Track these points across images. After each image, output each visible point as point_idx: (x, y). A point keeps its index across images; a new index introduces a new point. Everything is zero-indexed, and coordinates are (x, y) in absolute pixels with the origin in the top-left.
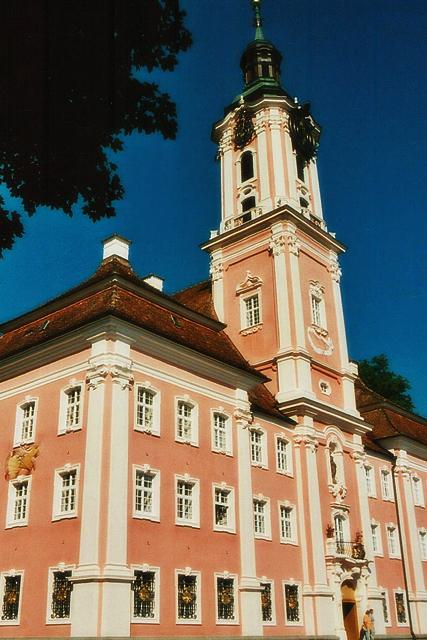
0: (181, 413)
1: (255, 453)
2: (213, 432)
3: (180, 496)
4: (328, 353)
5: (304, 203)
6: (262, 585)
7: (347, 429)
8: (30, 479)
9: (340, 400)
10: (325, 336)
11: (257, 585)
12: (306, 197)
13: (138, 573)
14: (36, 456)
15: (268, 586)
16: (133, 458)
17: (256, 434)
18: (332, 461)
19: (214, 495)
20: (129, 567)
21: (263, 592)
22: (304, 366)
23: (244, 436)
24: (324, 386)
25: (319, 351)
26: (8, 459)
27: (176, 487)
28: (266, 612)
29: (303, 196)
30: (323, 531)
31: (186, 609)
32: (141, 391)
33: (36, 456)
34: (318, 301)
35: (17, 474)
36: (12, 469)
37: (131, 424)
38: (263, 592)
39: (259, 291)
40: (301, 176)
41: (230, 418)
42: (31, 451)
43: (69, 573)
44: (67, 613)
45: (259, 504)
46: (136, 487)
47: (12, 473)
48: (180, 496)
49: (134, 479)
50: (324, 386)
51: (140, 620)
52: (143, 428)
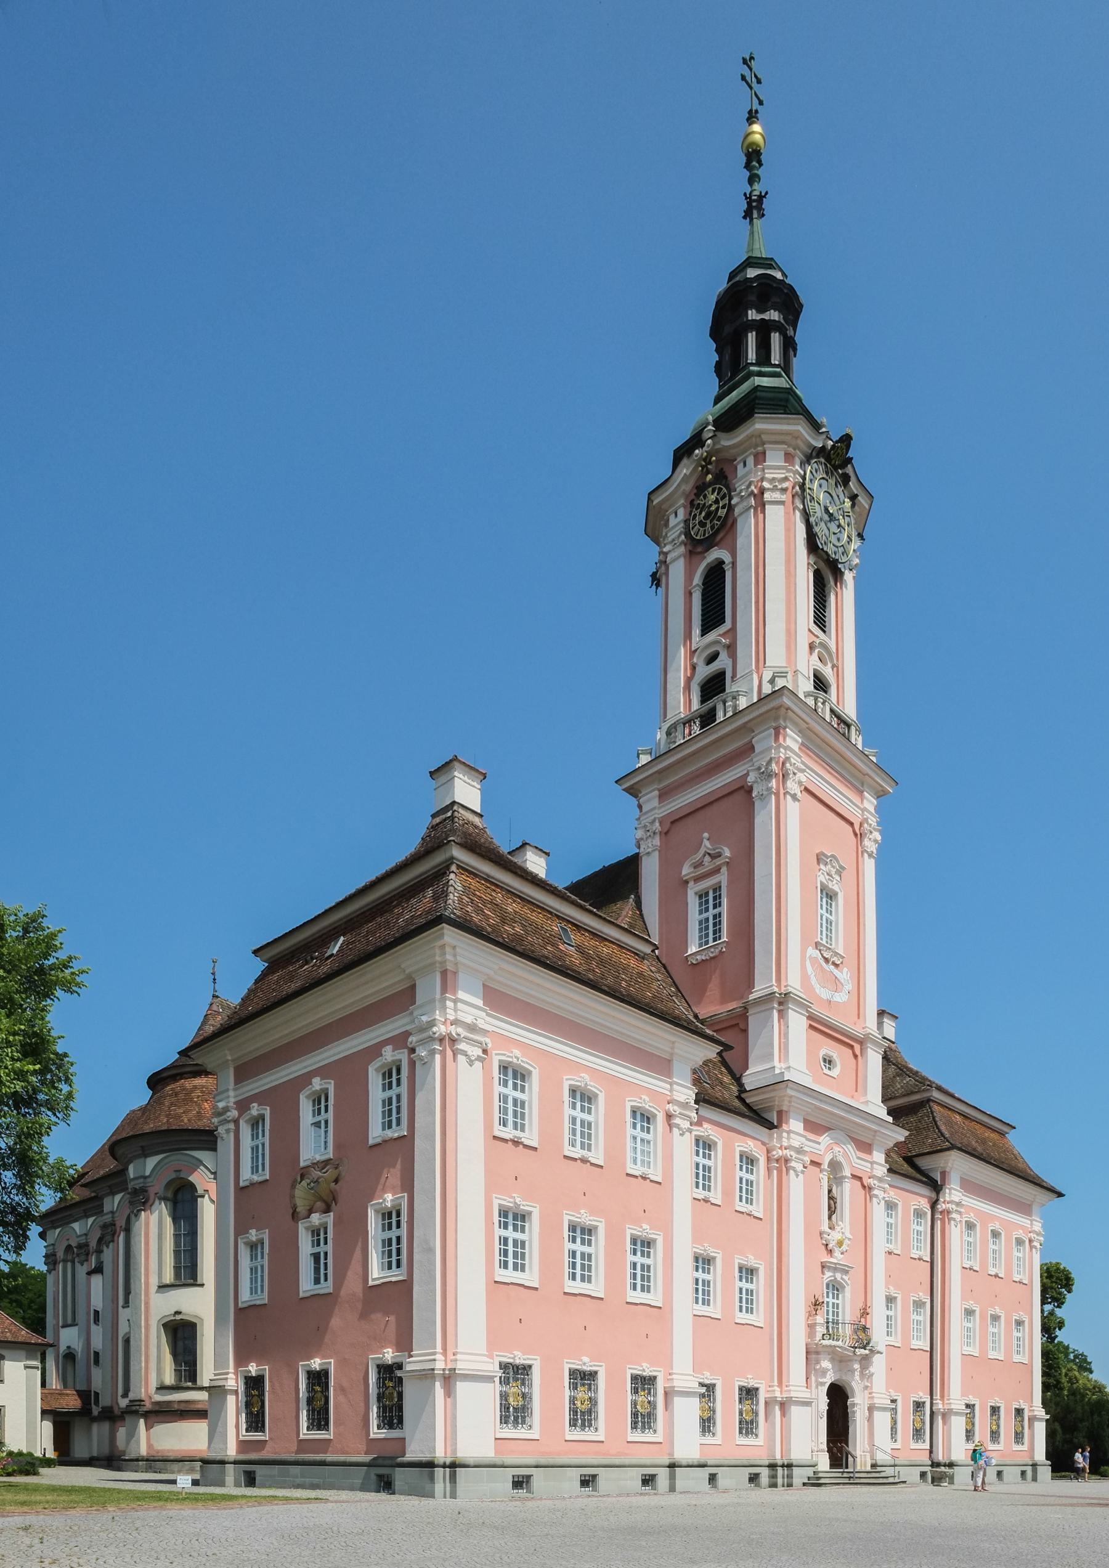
0: (574, 1108)
1: (703, 1177)
2: (629, 1140)
3: (573, 1246)
4: (841, 997)
5: (820, 683)
6: (702, 1385)
7: (865, 1147)
8: (330, 1219)
9: (859, 1084)
10: (836, 965)
11: (694, 1385)
12: (828, 672)
13: (504, 1366)
14: (336, 1181)
15: (710, 1388)
16: (491, 1186)
17: (705, 1145)
18: (830, 1191)
19: (628, 1246)
20: (491, 1356)
21: (703, 1396)
22: (797, 1022)
23: (683, 1147)
24: (829, 1061)
25: (824, 993)
26: (293, 1187)
28: (707, 1424)
29: (819, 666)
30: (806, 1300)
31: (582, 1417)
32: (504, 1068)
33: (336, 1181)
34: (831, 896)
35: (310, 1211)
36: (301, 1202)
37: (488, 1126)
38: (703, 1396)
39: (723, 878)
40: (820, 620)
41: (660, 1118)
42: (330, 1173)
43: (400, 1366)
44: (401, 1421)
45: (703, 1262)
46: (500, 1232)
47: (301, 1209)
48: (573, 1246)
49: (496, 1219)
50: (829, 1061)
51: (509, 1432)
52: (508, 1133)
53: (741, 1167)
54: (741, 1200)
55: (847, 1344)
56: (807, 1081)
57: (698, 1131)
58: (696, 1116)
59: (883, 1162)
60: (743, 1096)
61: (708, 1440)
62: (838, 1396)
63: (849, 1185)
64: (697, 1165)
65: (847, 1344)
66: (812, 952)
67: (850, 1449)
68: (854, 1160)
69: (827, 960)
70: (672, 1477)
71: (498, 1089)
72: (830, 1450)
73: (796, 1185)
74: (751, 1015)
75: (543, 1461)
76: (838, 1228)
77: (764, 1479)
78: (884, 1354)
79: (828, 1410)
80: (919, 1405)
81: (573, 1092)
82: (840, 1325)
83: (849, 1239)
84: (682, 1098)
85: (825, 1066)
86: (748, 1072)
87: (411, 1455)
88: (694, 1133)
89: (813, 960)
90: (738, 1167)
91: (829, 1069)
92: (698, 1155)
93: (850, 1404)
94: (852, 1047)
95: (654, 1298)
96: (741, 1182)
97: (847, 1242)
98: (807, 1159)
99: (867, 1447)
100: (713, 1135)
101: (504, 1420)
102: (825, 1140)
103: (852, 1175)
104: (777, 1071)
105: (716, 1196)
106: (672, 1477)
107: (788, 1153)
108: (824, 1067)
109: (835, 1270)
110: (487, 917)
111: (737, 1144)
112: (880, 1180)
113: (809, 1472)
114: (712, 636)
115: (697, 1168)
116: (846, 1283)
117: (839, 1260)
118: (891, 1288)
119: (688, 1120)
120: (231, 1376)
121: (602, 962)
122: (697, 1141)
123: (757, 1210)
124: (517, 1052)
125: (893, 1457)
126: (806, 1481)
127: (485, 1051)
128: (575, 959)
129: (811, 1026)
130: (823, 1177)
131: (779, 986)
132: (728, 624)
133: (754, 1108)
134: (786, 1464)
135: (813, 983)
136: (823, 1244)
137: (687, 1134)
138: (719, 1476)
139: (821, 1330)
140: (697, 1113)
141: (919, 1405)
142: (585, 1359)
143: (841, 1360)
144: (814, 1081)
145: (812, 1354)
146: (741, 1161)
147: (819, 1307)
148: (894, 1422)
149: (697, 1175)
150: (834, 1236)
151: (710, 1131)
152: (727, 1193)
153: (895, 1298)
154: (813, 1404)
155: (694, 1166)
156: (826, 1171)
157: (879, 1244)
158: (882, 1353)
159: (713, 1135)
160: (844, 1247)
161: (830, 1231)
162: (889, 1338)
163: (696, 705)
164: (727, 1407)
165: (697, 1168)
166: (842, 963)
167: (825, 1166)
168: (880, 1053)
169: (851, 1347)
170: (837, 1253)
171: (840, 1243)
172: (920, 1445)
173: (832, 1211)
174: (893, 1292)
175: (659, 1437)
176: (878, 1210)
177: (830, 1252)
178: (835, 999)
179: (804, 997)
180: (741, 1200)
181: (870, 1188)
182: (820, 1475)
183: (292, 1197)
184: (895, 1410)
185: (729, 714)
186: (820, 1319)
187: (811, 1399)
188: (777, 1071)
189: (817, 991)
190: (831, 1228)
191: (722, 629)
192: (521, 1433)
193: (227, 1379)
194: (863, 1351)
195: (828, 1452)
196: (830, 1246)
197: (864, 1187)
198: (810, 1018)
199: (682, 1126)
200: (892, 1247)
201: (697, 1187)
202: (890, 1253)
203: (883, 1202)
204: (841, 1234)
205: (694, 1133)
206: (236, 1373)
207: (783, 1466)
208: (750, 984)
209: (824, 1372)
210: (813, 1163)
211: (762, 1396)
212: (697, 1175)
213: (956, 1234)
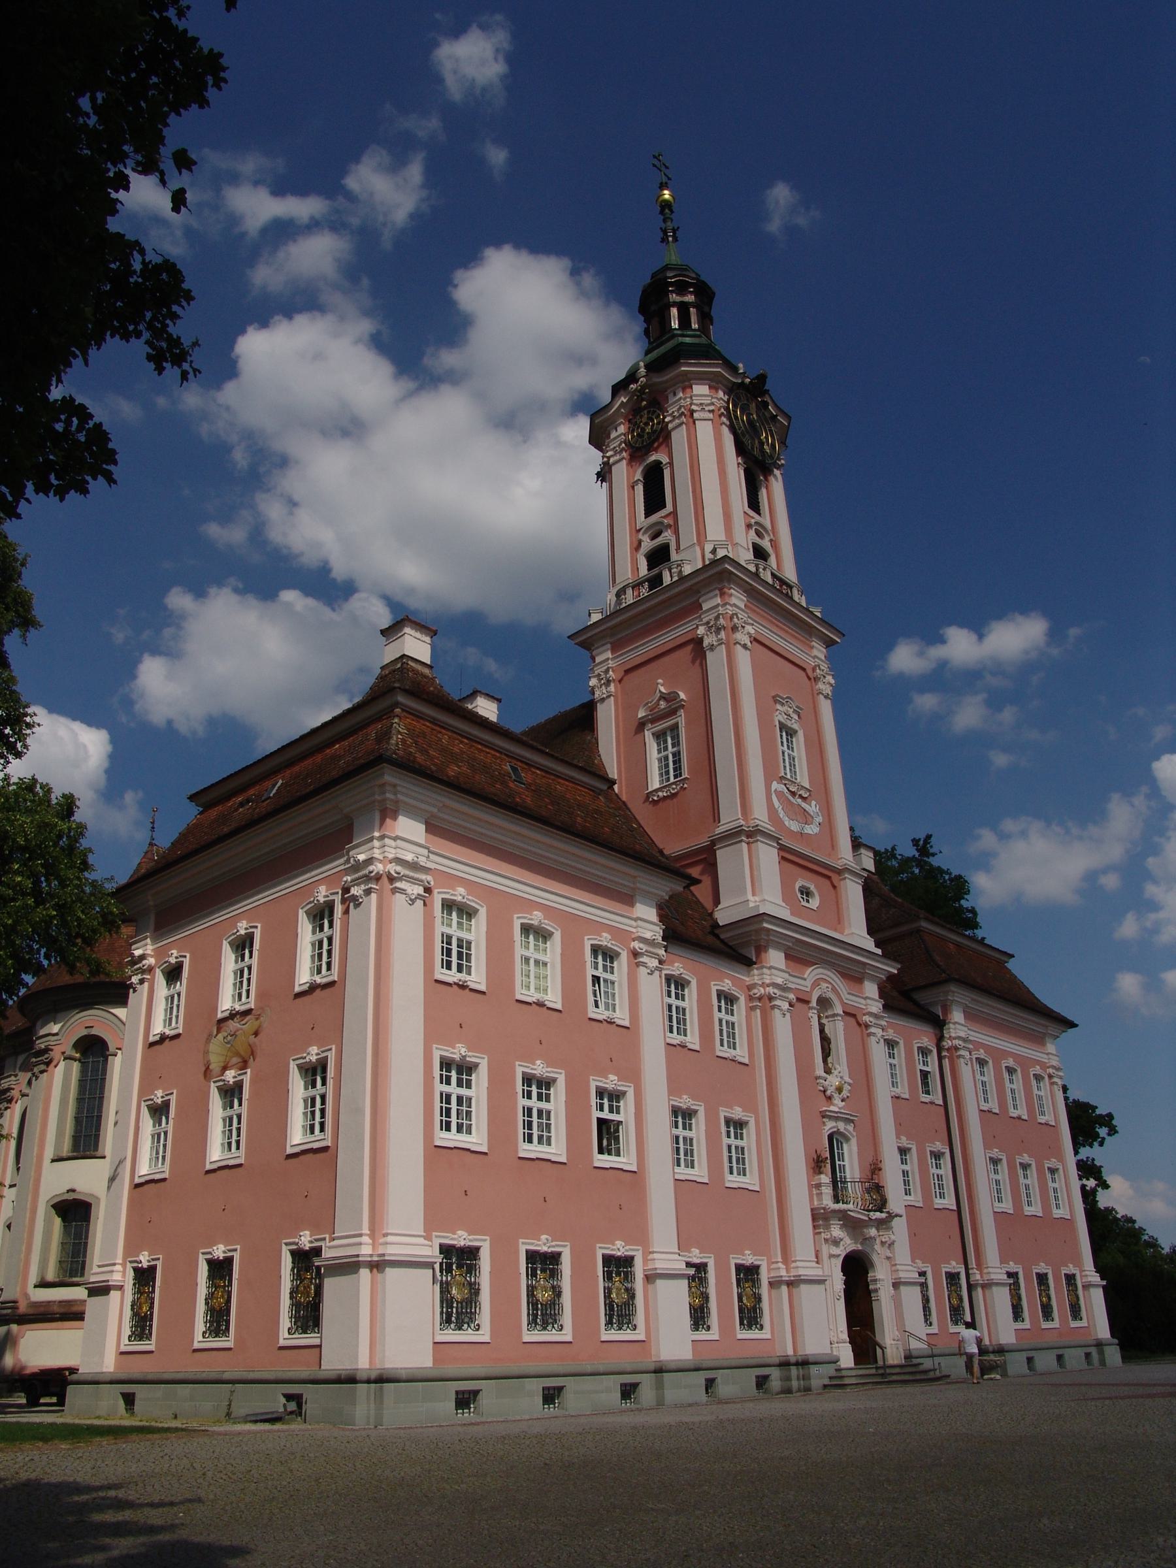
1: (675, 1020)
17: (677, 984)
18: (822, 1031)
22: (768, 855)
23: (651, 988)
24: (806, 892)
27: (519, 1087)
53: (720, 1007)
54: (722, 1045)
55: (859, 1207)
56: (785, 914)
57: (668, 970)
58: (664, 953)
59: (876, 996)
60: (717, 931)
63: (842, 1023)
64: (670, 1006)
65: (859, 1207)
67: (878, 1338)
68: (845, 996)
72: (852, 1341)
73: (783, 1026)
74: (719, 849)
76: (835, 1072)
77: (775, 1383)
78: (904, 1217)
79: (845, 1291)
82: (849, 1184)
83: (850, 1084)
84: (648, 935)
85: (803, 898)
86: (720, 907)
88: (664, 972)
90: (716, 1008)
91: (808, 901)
92: (669, 996)
93: (872, 1281)
94: (829, 878)
96: (721, 1025)
97: (846, 1088)
98: (792, 996)
99: (897, 1333)
100: (685, 974)
103: (844, 1012)
104: (751, 905)
105: (693, 1039)
108: (802, 900)
109: (837, 1119)
111: (713, 983)
112: (876, 1016)
113: (830, 1370)
115: (670, 1010)
116: (849, 1132)
117: (839, 1108)
118: (904, 1138)
119: (656, 958)
120: (119, 1268)
125: (929, 1344)
126: (827, 1382)
129: (783, 858)
130: (812, 1015)
133: (731, 944)
134: (800, 1361)
135: (781, 816)
136: (820, 1091)
137: (657, 973)
140: (666, 951)
143: (853, 1225)
144: (792, 914)
145: (819, 1217)
146: (719, 1001)
147: (823, 1164)
148: (926, 1300)
149: (670, 1017)
150: (833, 1081)
151: (682, 970)
153: (909, 1149)
154: (827, 1282)
155: (666, 1008)
156: (815, 1008)
158: (901, 1216)
159: (685, 974)
160: (845, 1093)
161: (825, 1075)
162: (908, 1197)
165: (670, 1010)
166: (810, 795)
167: (814, 1003)
168: (859, 884)
169: (864, 1210)
170: (837, 1100)
171: (839, 1090)
173: (826, 1053)
174: (904, 1142)
176: (878, 1051)
177: (829, 1098)
178: (806, 832)
179: (773, 829)
180: (722, 1045)
181: (867, 1026)
182: (844, 1373)
183: (206, 1052)
184: (924, 1286)
187: (824, 1276)
188: (751, 905)
189: (787, 823)
190: (828, 1071)
193: (112, 1271)
194: (878, 1215)
195: (850, 1343)
196: (828, 1093)
197: (859, 1025)
199: (650, 965)
200: (898, 1091)
201: (671, 1032)
202: (898, 1098)
203: (882, 1040)
204: (839, 1079)
205: (664, 972)
206: (124, 1265)
207: (797, 1364)
208: (716, 818)
209: (836, 1242)
210: (799, 1000)
211: (764, 1276)
212: (670, 1017)
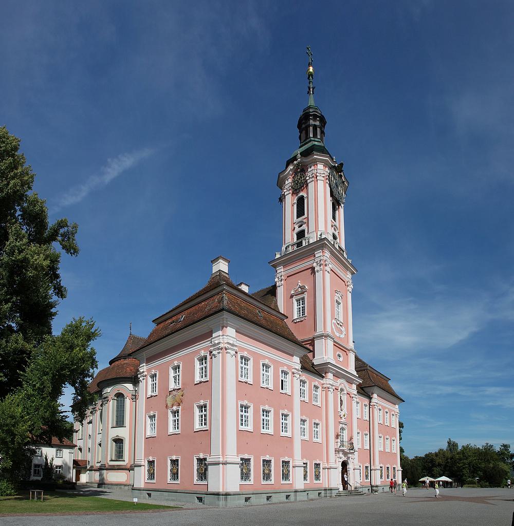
3: (263, 417)
7: (350, 381)
9: (346, 363)
13: (242, 459)
16: (238, 398)
17: (303, 382)
21: (304, 467)
22: (330, 343)
24: (339, 356)
31: (267, 476)
32: (242, 358)
38: (304, 467)
41: (290, 373)
45: (303, 421)
48: (263, 417)
51: (244, 483)
52: (243, 379)
61: (306, 482)
62: (344, 465)
66: (333, 321)
69: (338, 324)
70: (296, 496)
71: (240, 365)
73: (331, 396)
75: (255, 492)
80: (367, 467)
81: (263, 365)
87: (211, 490)
89: (334, 324)
95: (289, 434)
98: (334, 388)
101: (242, 478)
102: (340, 381)
105: (307, 399)
106: (296, 496)
107: (329, 386)
110: (236, 308)
114: (300, 219)
121: (271, 322)
122: (301, 381)
123: (319, 404)
124: (246, 353)
127: (236, 353)
128: (263, 322)
131: (325, 331)
132: (306, 215)
138: (309, 494)
139: (339, 444)
141: (367, 467)
142: (268, 456)
145: (337, 451)
152: (310, 399)
157: (355, 417)
160: (345, 417)
163: (295, 240)
164: (311, 470)
167: (339, 390)
172: (367, 481)
175: (291, 482)
185: (307, 244)
186: (339, 440)
190: (342, 410)
191: (303, 217)
192: (247, 482)
198: (334, 342)
211: (321, 466)
213: (376, 412)
